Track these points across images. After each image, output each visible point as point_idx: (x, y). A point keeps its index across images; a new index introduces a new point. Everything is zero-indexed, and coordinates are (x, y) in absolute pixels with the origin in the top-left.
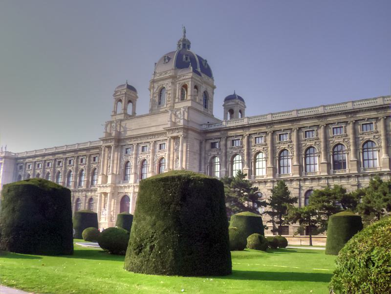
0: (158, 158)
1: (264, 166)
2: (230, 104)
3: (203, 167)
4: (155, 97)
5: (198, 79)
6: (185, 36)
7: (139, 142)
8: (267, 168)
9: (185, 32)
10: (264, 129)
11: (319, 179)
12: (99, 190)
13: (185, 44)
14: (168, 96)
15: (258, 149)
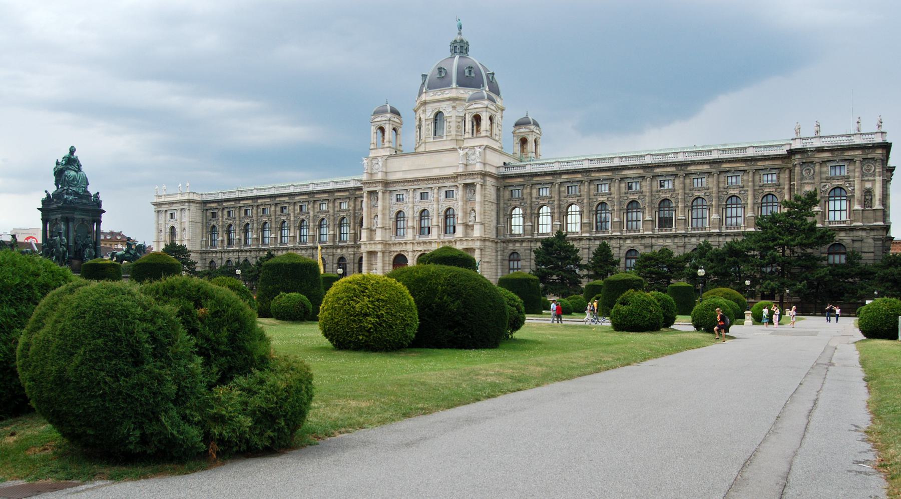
0: (445, 209)
1: (578, 220)
2: (522, 130)
3: (501, 220)
4: (428, 125)
5: (493, 107)
6: (460, 34)
7: (418, 187)
8: (582, 224)
9: (461, 28)
10: (579, 177)
11: (643, 237)
12: (364, 249)
13: (460, 48)
14: (448, 124)
15: (571, 200)
